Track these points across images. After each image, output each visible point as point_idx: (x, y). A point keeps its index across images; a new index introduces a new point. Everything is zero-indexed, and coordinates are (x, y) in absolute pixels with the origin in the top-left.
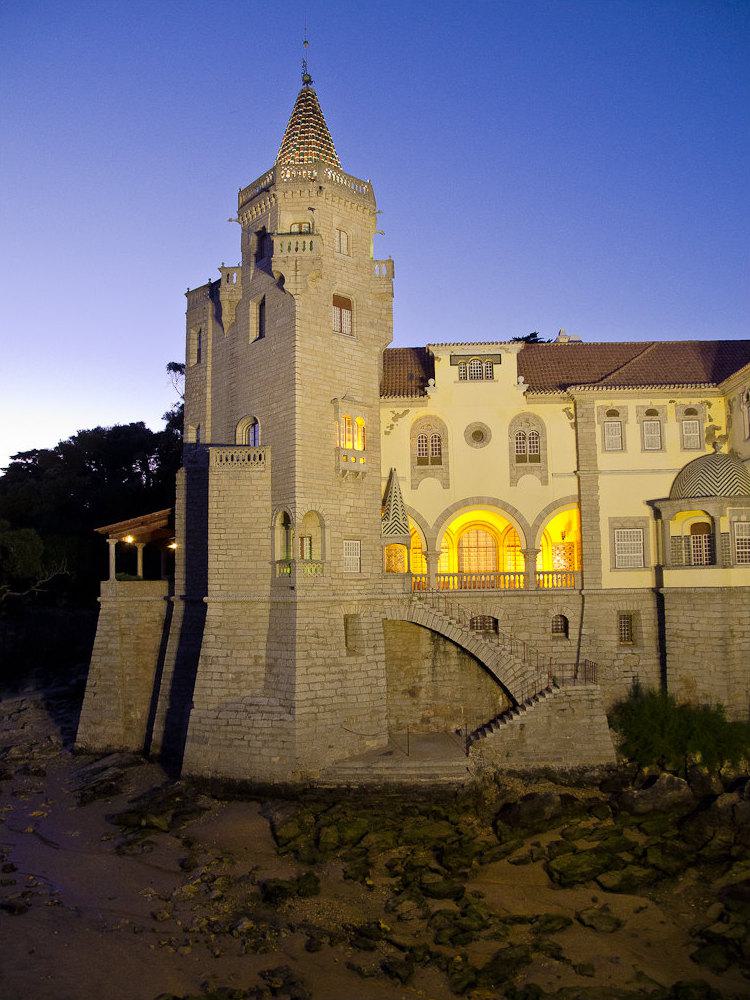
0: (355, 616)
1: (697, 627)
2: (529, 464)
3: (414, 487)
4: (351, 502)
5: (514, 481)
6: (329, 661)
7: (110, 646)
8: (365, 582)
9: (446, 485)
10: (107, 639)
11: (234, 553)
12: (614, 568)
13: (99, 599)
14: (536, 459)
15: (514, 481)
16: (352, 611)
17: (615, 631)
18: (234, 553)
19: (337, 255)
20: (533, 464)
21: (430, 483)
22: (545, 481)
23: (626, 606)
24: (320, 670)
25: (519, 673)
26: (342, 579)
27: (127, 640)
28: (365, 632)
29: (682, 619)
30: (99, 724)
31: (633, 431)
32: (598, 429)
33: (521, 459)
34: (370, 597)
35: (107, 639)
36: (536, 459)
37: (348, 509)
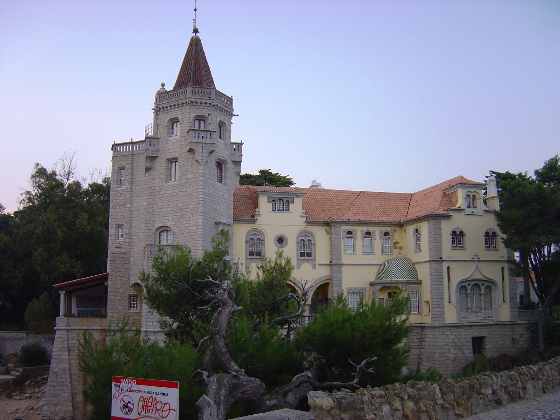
7: (63, 357)
10: (60, 353)
13: (55, 328)
22: (314, 267)
27: (72, 353)
30: (58, 405)
35: (60, 353)
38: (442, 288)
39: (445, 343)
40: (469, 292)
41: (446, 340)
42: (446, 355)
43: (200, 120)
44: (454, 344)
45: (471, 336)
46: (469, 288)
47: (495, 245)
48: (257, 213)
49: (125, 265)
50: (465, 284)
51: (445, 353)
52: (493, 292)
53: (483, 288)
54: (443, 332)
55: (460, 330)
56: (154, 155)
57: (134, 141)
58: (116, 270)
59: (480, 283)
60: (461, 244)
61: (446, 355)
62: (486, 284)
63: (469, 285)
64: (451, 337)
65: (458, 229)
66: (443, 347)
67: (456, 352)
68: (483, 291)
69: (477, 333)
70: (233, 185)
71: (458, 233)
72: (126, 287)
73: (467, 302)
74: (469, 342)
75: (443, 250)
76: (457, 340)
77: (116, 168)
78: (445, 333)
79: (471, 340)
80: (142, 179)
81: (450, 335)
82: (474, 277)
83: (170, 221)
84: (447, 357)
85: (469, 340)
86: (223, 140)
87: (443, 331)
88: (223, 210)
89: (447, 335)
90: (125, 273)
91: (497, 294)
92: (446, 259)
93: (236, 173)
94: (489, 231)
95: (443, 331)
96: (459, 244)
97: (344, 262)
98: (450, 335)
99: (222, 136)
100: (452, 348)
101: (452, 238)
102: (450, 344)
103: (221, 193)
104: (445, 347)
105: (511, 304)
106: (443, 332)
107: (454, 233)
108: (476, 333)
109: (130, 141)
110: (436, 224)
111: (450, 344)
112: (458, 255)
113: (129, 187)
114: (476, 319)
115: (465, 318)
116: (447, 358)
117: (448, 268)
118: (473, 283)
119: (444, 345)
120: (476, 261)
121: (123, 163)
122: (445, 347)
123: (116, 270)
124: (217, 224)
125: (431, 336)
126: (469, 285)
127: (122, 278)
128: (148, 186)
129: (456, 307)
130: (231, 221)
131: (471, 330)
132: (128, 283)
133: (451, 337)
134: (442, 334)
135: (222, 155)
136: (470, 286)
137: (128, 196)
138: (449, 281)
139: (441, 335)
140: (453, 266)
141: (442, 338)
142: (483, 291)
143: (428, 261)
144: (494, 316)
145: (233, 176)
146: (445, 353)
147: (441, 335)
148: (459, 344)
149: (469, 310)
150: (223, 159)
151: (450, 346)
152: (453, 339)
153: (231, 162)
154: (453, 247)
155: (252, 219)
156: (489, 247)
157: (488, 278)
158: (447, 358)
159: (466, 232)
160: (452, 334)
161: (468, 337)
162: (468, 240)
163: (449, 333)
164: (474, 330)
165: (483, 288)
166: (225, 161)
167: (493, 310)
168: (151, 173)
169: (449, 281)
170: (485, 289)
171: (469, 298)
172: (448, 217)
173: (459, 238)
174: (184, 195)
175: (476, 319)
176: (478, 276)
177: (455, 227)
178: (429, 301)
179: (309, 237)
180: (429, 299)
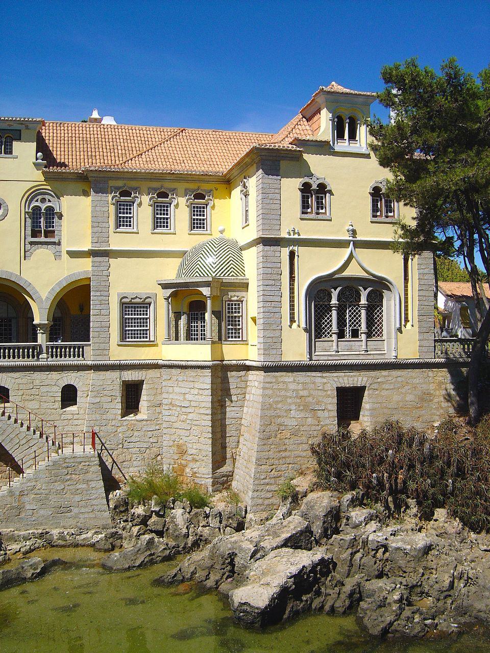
41: (283, 393)
61: (279, 420)
67: (302, 415)
76: (305, 393)
84: (280, 425)
89: (284, 382)
94: (380, 185)
97: (113, 247)
100: (293, 407)
102: (289, 400)
133: (292, 386)
148: (310, 399)
152: (297, 390)
160: (294, 381)
161: (328, 387)
176: (353, 271)
179: (49, 201)
180: (255, 314)
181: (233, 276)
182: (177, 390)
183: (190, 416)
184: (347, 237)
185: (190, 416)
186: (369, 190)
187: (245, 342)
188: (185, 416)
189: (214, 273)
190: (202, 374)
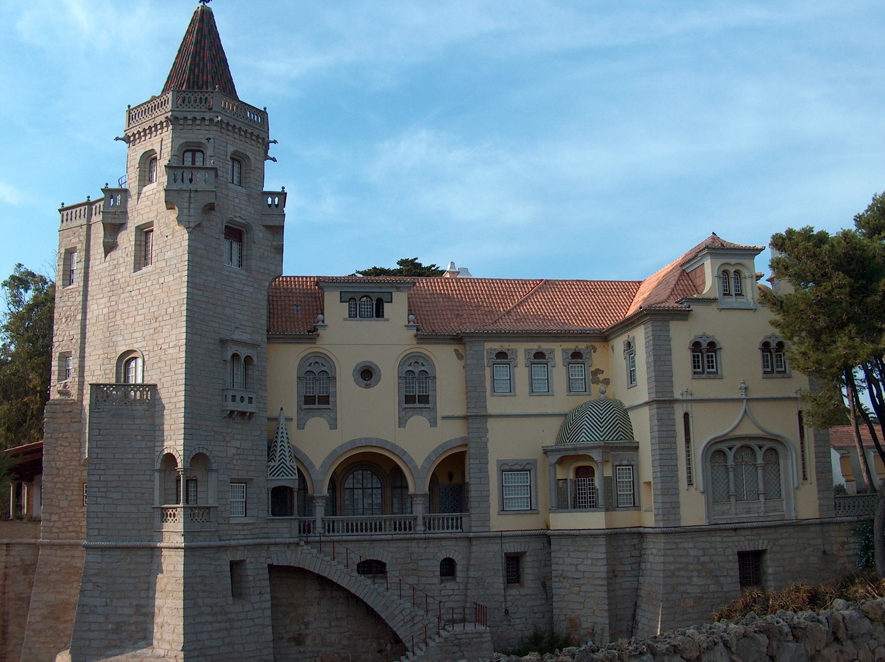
0: (242, 562)
1: (581, 568)
2: (417, 405)
3: (301, 427)
4: (238, 444)
5: (402, 422)
6: (216, 609)
8: (251, 527)
9: (333, 425)
11: (114, 495)
12: (503, 510)
14: (424, 399)
15: (402, 422)
16: (238, 557)
17: (501, 573)
18: (114, 495)
19: (230, 185)
20: (422, 405)
21: (317, 424)
23: (512, 547)
24: (209, 618)
25: (408, 618)
26: (228, 524)
28: (251, 578)
29: (568, 561)
31: (521, 373)
32: (488, 371)
33: (409, 399)
34: (256, 541)
36: (424, 399)
37: (234, 451)
38: (674, 456)
39: (681, 566)
40: (730, 462)
42: (682, 588)
43: (194, 152)
44: (700, 567)
45: (736, 550)
46: (730, 455)
47: (785, 369)
48: (320, 323)
49: (72, 425)
50: (723, 446)
51: (681, 584)
52: (781, 461)
53: (760, 455)
54: (676, 543)
55: (714, 539)
56: (117, 222)
57: (92, 200)
58: (56, 435)
59: (753, 444)
60: (713, 367)
61: (682, 588)
62: (767, 445)
63: (730, 449)
64: (693, 552)
65: (704, 338)
66: (676, 573)
68: (760, 461)
69: (748, 544)
70: (266, 271)
71: (704, 345)
72: (74, 465)
73: (728, 482)
74: (730, 561)
75: (674, 379)
76: (706, 559)
77: (63, 251)
78: (680, 546)
79: (736, 557)
80: (101, 267)
81: (691, 548)
82: (743, 431)
83: (139, 340)
85: (731, 558)
86: (245, 188)
87: (676, 540)
88: (240, 316)
89: (684, 549)
90: (73, 440)
91: (790, 466)
92: (680, 397)
93: (274, 248)
94: (769, 340)
95: (676, 540)
96: (709, 367)
98: (691, 548)
99: (243, 180)
100: (695, 574)
101: (694, 356)
102: (691, 567)
103: (237, 285)
104: (681, 573)
105: (818, 485)
106: (676, 543)
107: (696, 346)
108: (746, 543)
109: (85, 200)
110: (659, 328)
111: (691, 567)
112: (705, 388)
113: (82, 284)
114: (748, 515)
115: (723, 513)
116: (685, 596)
117: (686, 416)
118: (738, 444)
119: (679, 569)
120: (745, 401)
121: (73, 241)
122: (681, 573)
123: (56, 435)
124: (223, 342)
125: (655, 551)
126: (730, 449)
127: (66, 450)
128: (108, 280)
129: (703, 493)
130: (261, 337)
131: (736, 539)
132: (78, 459)
133: (693, 552)
134: (674, 547)
135: (238, 215)
136: (734, 450)
137: (80, 298)
138: (688, 440)
139: (671, 549)
140: (696, 412)
141: (673, 556)
142: (760, 461)
143: (647, 403)
144: (785, 509)
145: (266, 254)
146: (681, 584)
147: (671, 549)
148: (712, 565)
149: (733, 499)
150: (243, 221)
151: (692, 571)
153: (262, 228)
154: (695, 373)
155: (312, 334)
156: (772, 372)
157: (767, 433)
158: (685, 596)
159: (721, 340)
160: (695, 547)
161: (729, 551)
162: (726, 359)
163: (691, 545)
164: (743, 538)
165: (760, 455)
166: (248, 227)
167: (783, 496)
168: (114, 254)
169: (688, 440)
170: (765, 454)
171: (731, 474)
172: (683, 315)
173: (708, 356)
174: (160, 291)
175: (748, 515)
176: (748, 430)
177: (700, 333)
178: (650, 482)
181: (621, 439)
182: (568, 561)
183: (584, 588)
184: (740, 395)
185: (584, 588)
186: (758, 344)
187: (534, 512)
188: (578, 588)
189: (602, 437)
190: (595, 544)
